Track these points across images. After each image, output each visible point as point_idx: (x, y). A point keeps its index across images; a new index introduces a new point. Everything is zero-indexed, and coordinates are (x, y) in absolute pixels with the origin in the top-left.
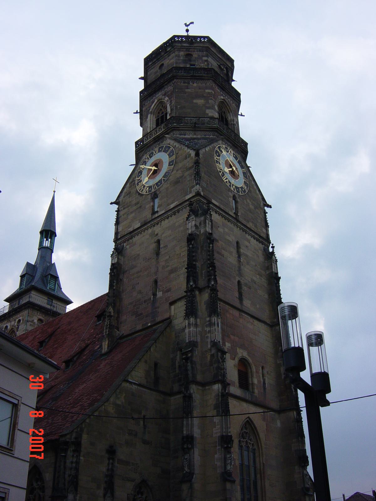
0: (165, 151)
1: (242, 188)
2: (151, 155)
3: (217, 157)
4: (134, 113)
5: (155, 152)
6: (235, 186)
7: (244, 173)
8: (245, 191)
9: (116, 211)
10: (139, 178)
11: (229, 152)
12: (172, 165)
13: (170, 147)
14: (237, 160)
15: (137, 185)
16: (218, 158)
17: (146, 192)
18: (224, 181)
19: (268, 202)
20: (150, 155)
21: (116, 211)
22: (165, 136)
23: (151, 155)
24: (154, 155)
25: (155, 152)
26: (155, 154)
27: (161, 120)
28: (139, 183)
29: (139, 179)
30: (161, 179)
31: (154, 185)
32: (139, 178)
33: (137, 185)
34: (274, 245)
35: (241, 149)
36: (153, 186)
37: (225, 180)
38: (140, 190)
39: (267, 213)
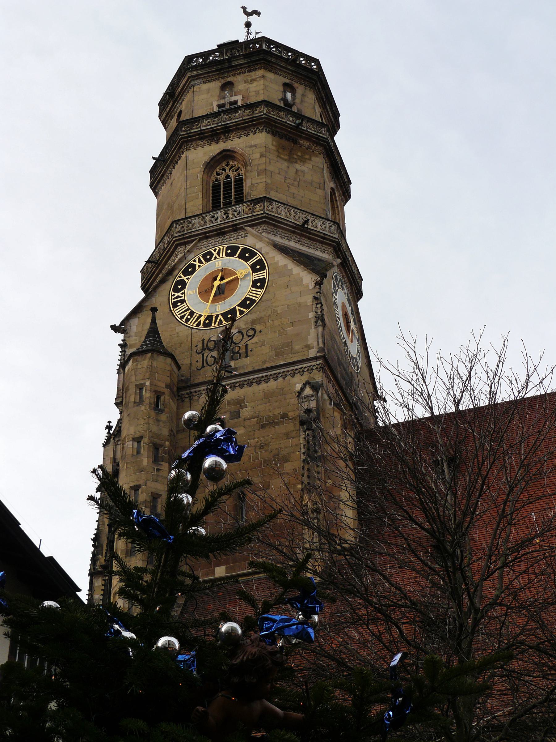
2: (208, 257)
5: (219, 254)
12: (261, 287)
17: (198, 325)
20: (204, 256)
22: (245, 228)
23: (208, 257)
25: (219, 254)
27: (224, 192)
28: (179, 304)
29: (178, 297)
32: (179, 294)
34: (111, 424)
36: (214, 316)
38: (182, 318)
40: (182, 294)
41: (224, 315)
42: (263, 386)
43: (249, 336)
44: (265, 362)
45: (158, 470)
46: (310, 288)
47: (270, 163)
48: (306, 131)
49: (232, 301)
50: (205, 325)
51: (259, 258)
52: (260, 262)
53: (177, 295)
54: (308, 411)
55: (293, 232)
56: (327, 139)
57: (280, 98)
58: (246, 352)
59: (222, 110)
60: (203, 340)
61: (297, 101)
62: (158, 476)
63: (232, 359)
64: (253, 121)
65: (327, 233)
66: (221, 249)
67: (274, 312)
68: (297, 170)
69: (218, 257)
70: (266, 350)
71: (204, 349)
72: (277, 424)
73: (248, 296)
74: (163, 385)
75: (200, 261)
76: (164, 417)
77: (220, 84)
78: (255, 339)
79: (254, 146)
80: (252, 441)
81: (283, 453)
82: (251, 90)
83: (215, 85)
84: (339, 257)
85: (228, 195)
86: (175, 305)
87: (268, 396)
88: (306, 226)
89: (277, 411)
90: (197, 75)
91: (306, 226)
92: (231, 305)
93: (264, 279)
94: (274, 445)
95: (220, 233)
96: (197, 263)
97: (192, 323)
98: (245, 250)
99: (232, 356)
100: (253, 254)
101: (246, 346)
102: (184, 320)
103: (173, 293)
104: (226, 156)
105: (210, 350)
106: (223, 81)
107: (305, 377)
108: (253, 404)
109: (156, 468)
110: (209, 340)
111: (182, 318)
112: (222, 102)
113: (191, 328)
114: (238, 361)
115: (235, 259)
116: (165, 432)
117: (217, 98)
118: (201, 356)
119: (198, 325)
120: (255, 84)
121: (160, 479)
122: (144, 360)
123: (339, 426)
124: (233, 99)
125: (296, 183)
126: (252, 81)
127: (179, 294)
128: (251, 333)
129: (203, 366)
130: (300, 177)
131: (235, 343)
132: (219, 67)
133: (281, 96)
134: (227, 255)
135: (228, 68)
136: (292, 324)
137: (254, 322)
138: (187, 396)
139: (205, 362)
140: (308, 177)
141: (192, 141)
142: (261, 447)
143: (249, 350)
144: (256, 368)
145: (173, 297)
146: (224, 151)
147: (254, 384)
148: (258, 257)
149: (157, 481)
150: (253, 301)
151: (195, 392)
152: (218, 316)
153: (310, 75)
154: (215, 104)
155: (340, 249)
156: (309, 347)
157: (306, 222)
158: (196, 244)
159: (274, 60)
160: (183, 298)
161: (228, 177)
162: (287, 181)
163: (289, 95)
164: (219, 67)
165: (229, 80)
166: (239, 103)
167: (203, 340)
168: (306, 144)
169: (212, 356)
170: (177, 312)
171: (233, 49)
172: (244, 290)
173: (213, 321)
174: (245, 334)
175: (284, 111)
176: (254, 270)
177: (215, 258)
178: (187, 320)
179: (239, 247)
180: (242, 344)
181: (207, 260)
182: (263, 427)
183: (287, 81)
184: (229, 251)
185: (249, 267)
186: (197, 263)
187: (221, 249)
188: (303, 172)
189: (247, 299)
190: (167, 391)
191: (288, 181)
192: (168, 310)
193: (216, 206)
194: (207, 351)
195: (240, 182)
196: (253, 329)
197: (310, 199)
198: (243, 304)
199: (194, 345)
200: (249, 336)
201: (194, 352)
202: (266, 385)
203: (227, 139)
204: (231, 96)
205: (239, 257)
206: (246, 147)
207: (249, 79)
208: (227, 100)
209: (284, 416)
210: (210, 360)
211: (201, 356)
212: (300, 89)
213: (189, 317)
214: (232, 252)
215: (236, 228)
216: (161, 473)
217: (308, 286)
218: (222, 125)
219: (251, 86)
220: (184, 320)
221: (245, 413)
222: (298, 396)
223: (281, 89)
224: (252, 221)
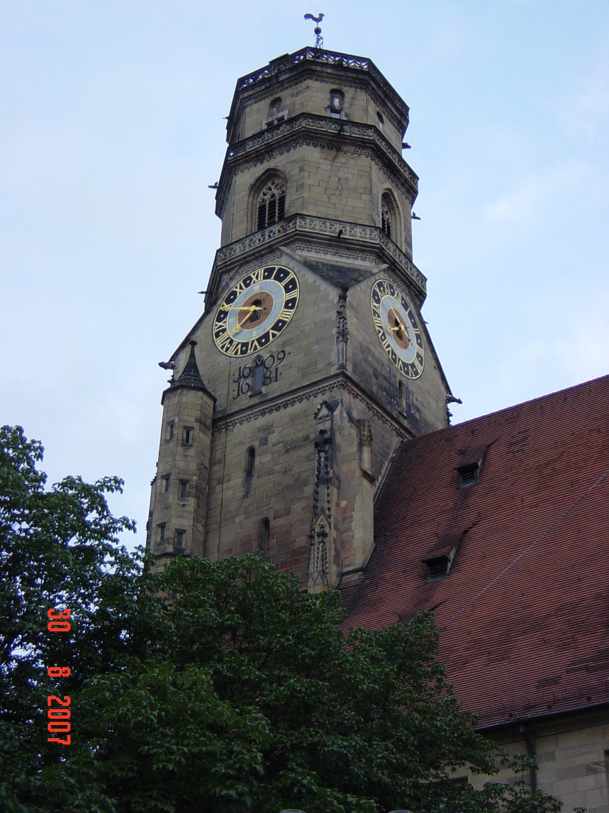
0: (278, 279)
1: (413, 365)
2: (248, 282)
3: (376, 303)
4: (210, 187)
5: (257, 278)
6: (402, 362)
7: (418, 337)
8: (416, 373)
9: (169, 381)
10: (220, 322)
11: (396, 295)
12: (292, 308)
13: (289, 273)
14: (406, 310)
15: (216, 337)
16: (377, 305)
17: (236, 353)
18: (384, 351)
19: (455, 395)
20: (244, 282)
21: (169, 381)
22: (281, 248)
23: (248, 282)
24: (254, 282)
25: (257, 278)
26: (256, 281)
28: (221, 333)
30: (268, 333)
31: (253, 342)
33: (216, 337)
35: (415, 290)
36: (250, 343)
37: (387, 347)
38: (222, 347)
39: (451, 415)
40: (224, 323)
41: (259, 340)
42: (290, 409)
44: (292, 384)
45: (184, 506)
46: (336, 302)
47: (309, 176)
48: (350, 136)
49: (266, 325)
50: (243, 352)
51: (292, 277)
52: (293, 281)
53: (220, 324)
54: (322, 432)
55: (329, 245)
56: (374, 140)
57: (326, 106)
58: (276, 377)
59: (271, 127)
60: (240, 368)
61: (346, 105)
62: (184, 511)
63: (264, 384)
64: (293, 136)
65: (368, 240)
66: (260, 272)
68: (340, 179)
69: (256, 281)
70: (294, 372)
71: (240, 378)
72: (300, 447)
73: (281, 318)
74: (193, 419)
75: (241, 288)
76: (191, 452)
77: (269, 102)
79: (295, 160)
80: (277, 467)
81: (303, 476)
82: (297, 103)
83: (265, 104)
84: (385, 262)
85: (272, 216)
86: (217, 335)
87: (293, 419)
88: (342, 236)
89: (300, 435)
90: (249, 96)
91: (342, 236)
92: (265, 329)
93: (295, 299)
94: (296, 470)
95: (257, 256)
96: (238, 290)
97: (231, 353)
98: (280, 271)
99: (264, 382)
100: (287, 274)
101: (277, 369)
102: (224, 349)
103: (217, 323)
104: (271, 175)
105: (245, 377)
106: (272, 98)
107: (320, 399)
108: (280, 429)
109: (181, 503)
110: (245, 368)
111: (222, 347)
112: (270, 120)
113: (230, 357)
114: (269, 386)
115: (271, 280)
116: (193, 466)
117: (266, 116)
118: (237, 383)
119: (236, 353)
121: (185, 514)
122: (175, 396)
123: (356, 443)
124: (280, 115)
125: (338, 192)
126: (298, 93)
127: (221, 324)
128: (281, 356)
129: (238, 395)
130: (344, 186)
131: (267, 368)
132: (268, 84)
133: (328, 103)
134: (265, 278)
135: (276, 83)
136: (317, 342)
138: (223, 427)
139: (240, 391)
140: (352, 184)
141: (239, 164)
142: (285, 472)
143: (278, 373)
144: (284, 392)
145: (216, 327)
146: (268, 170)
147: (282, 408)
148: (292, 275)
149: (182, 517)
150: (284, 323)
151: (231, 422)
152: (253, 342)
153: (360, 76)
154: (264, 122)
155: (384, 254)
156: (330, 364)
157: (341, 232)
158: (237, 271)
159: (319, 68)
160: (224, 327)
161: (273, 196)
162: (327, 192)
163: (337, 102)
164: (268, 84)
165: (277, 96)
166: (286, 118)
167: (240, 368)
168: (352, 149)
169: (247, 384)
170: (219, 342)
171: (279, 65)
172: (278, 312)
173: (249, 347)
174: (276, 358)
175: (325, 120)
176: (287, 290)
177: (254, 282)
178: (227, 349)
179: (274, 269)
180: (273, 369)
181: (247, 285)
182: (287, 451)
183: (335, 87)
184: (266, 274)
185: (283, 288)
186: (238, 290)
187: (260, 272)
188: (347, 179)
189: (279, 321)
190: (197, 426)
192: (211, 341)
193: (261, 226)
194: (242, 379)
195: (282, 199)
196: (283, 352)
197: (353, 207)
198: (276, 327)
199: (232, 374)
200: (280, 359)
201: (231, 380)
202: (293, 407)
203: (271, 157)
205: (275, 279)
206: (287, 163)
207: (296, 91)
208: (275, 117)
209: (306, 438)
210: (245, 387)
211: (237, 383)
212: (349, 92)
213: (229, 346)
214: (269, 273)
215: (272, 249)
216: (186, 508)
217: (333, 301)
218: (265, 145)
219: (296, 98)
220: (224, 349)
221: (273, 438)
222: (315, 417)
223: (328, 96)
224: (286, 240)
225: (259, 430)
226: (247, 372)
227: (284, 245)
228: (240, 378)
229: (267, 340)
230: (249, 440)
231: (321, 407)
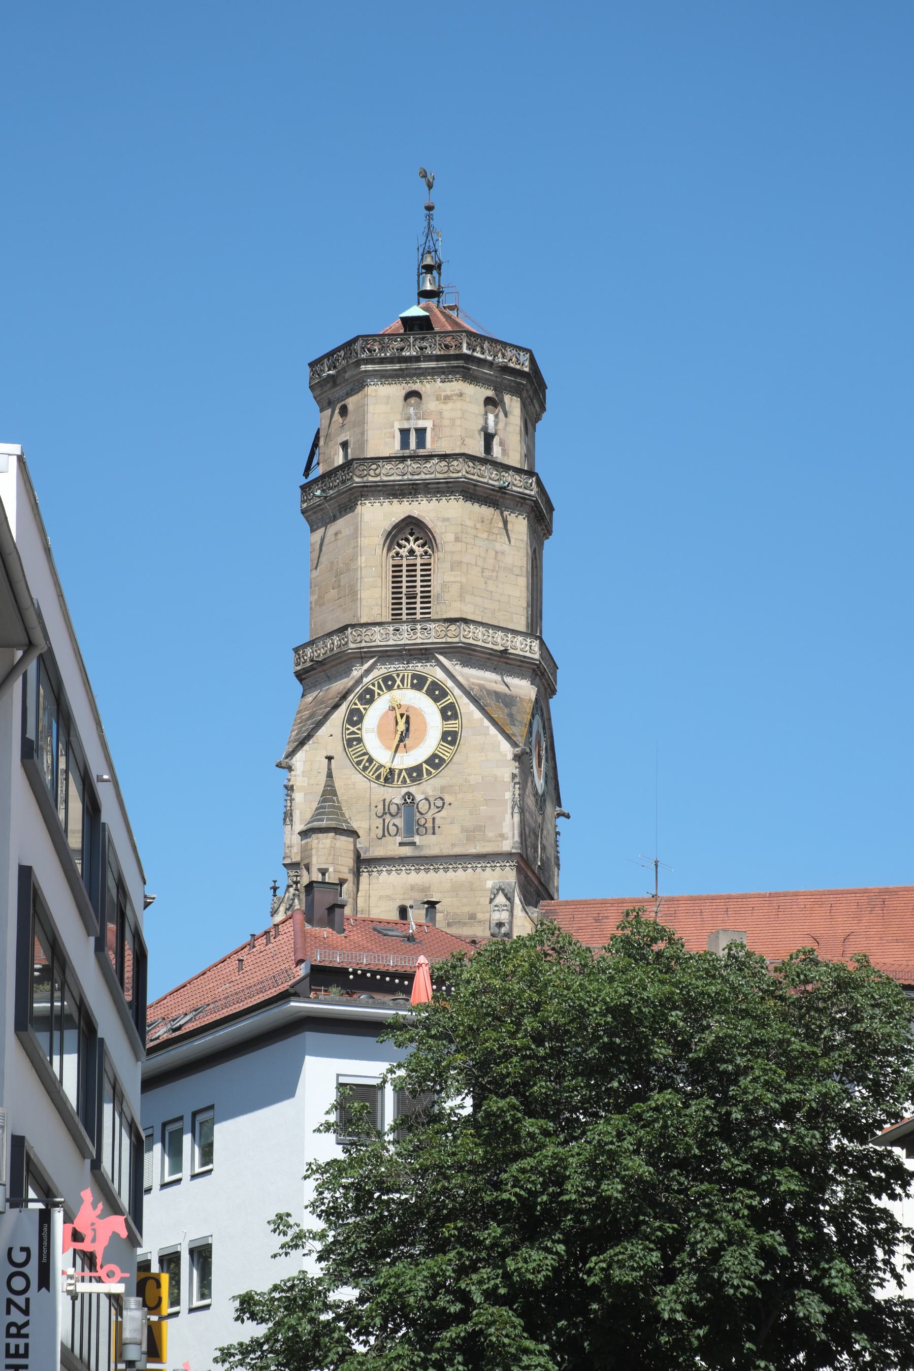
5: (402, 681)
29: (353, 733)
30: (421, 765)
36: (397, 772)
43: (438, 807)
44: (453, 845)
53: (352, 729)
54: (500, 925)
58: (434, 827)
60: (384, 801)
67: (466, 781)
70: (456, 830)
71: (385, 813)
72: (465, 924)
74: (346, 870)
78: (443, 813)
82: (446, 414)
89: (466, 909)
101: (434, 819)
104: (412, 527)
117: (399, 416)
120: (450, 405)
126: (447, 398)
127: (354, 729)
129: (384, 836)
136: (487, 802)
137: (443, 789)
139: (386, 831)
147: (441, 871)
150: (442, 760)
169: (394, 825)
173: (396, 777)
180: (429, 816)
191: (487, 573)
196: (442, 799)
197: (509, 596)
200: (438, 807)
204: (419, 419)
209: (472, 917)
210: (393, 830)
211: (381, 820)
214: (419, 682)
217: (505, 755)
220: (361, 767)
223: (481, 409)
225: (412, 888)
226: (394, 809)
227: (441, 654)
228: (385, 813)
229: (420, 775)
230: (402, 897)
231: (498, 893)
